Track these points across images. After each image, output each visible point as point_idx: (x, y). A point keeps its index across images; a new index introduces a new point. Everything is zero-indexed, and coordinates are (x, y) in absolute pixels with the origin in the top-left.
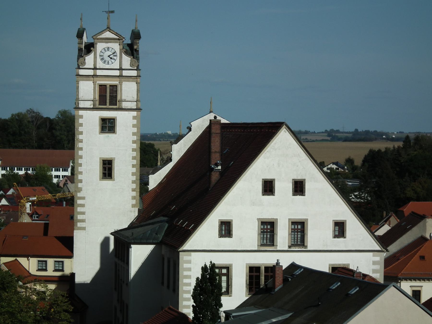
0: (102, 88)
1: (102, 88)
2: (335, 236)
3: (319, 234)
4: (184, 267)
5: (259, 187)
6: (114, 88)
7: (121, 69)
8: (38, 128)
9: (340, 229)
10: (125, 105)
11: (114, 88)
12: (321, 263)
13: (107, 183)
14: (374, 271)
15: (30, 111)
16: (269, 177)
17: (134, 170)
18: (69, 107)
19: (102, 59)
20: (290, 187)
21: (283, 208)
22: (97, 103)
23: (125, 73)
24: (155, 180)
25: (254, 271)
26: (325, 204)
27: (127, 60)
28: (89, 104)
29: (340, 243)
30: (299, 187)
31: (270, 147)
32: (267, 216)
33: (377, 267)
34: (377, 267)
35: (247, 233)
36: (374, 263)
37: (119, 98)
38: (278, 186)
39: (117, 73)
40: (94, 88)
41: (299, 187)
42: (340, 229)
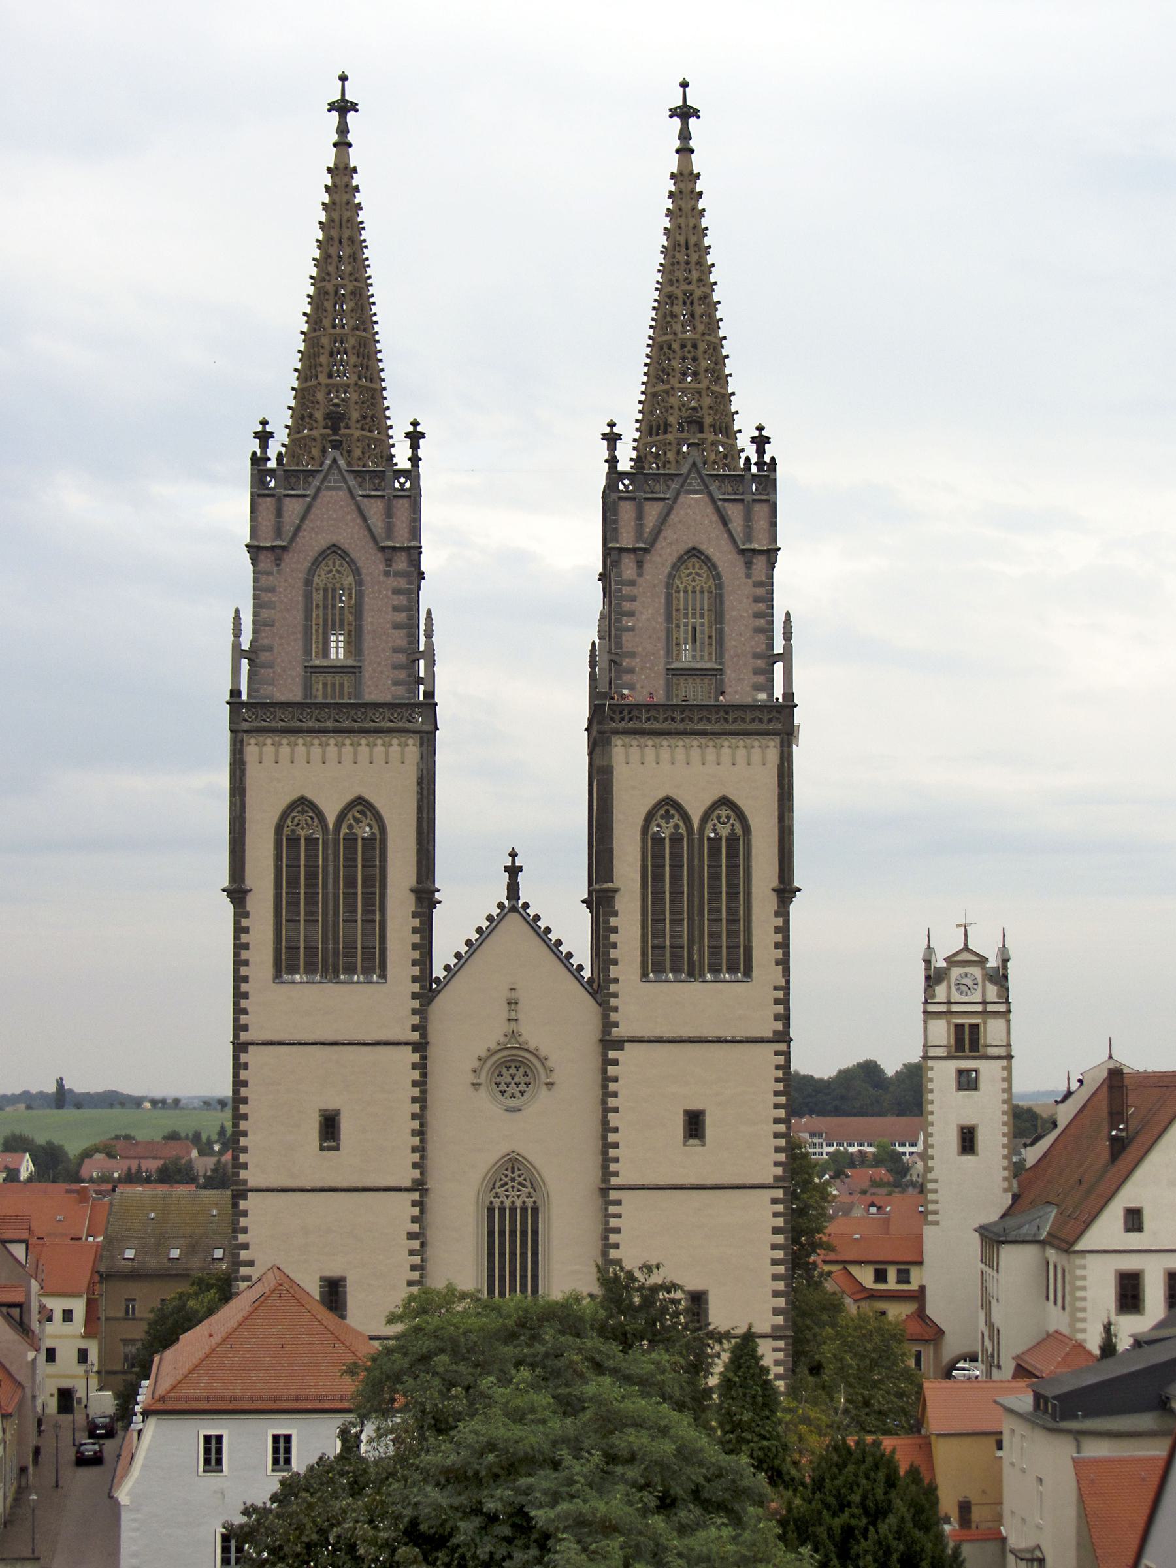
0: (959, 1028)
1: (959, 1028)
6: (975, 1028)
7: (984, 1003)
11: (975, 1028)
17: (1006, 1140)
22: (953, 1049)
23: (990, 1008)
24: (1032, 1155)
27: (992, 991)
37: (982, 1042)
39: (979, 1008)
40: (948, 1029)
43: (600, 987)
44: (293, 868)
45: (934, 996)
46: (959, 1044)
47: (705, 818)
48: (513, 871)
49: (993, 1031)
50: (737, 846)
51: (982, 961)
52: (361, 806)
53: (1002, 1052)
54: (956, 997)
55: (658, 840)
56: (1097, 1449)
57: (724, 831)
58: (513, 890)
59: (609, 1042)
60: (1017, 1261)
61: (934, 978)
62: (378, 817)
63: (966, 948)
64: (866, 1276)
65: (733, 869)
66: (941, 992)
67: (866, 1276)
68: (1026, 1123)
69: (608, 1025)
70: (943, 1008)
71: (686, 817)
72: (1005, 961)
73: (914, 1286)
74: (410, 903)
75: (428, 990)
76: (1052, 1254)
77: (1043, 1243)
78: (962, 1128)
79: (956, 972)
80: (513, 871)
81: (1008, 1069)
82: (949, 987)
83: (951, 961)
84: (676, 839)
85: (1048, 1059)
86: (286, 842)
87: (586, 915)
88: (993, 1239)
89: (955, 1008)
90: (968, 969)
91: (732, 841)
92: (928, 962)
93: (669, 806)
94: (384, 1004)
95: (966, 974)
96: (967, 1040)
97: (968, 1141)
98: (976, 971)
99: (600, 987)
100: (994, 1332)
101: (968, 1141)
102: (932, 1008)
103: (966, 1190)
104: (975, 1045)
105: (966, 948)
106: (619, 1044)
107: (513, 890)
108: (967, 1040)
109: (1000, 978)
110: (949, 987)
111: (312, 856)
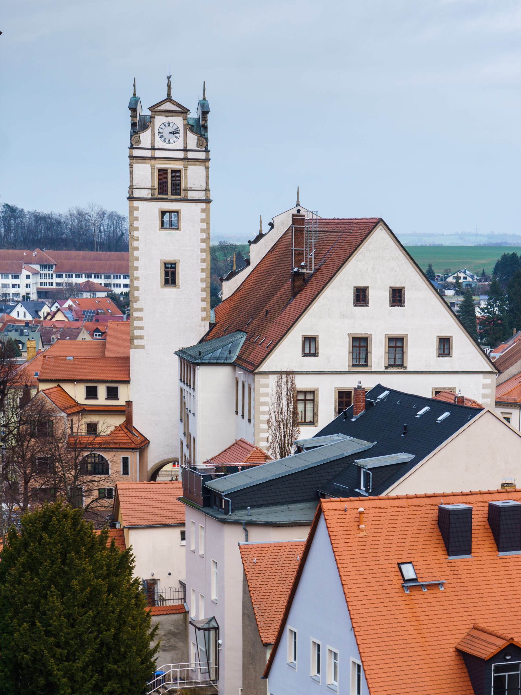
0: (162, 172)
1: (162, 172)
2: (440, 356)
3: (420, 353)
4: (261, 392)
5: (351, 295)
7: (185, 150)
9: (445, 346)
10: (191, 195)
11: (176, 173)
12: (421, 387)
13: (170, 291)
14: (484, 396)
16: (362, 284)
17: (204, 275)
19: (162, 137)
20: (387, 295)
21: (379, 321)
22: (157, 192)
23: (190, 155)
24: (228, 289)
25: (344, 397)
26: (427, 318)
27: (192, 140)
28: (146, 194)
29: (445, 364)
30: (397, 297)
31: (363, 247)
32: (360, 331)
33: (488, 391)
34: (488, 391)
35: (336, 352)
36: (485, 386)
37: (183, 186)
38: (372, 295)
39: (181, 155)
40: (153, 173)
41: (397, 297)
42: (445, 346)
45: (138, 142)
46: (162, 188)
49: (193, 177)
51: (183, 111)
53: (202, 196)
54: (159, 143)
56: (260, 537)
60: (213, 381)
61: (139, 126)
63: (169, 99)
64: (78, 393)
66: (145, 138)
67: (78, 393)
68: (224, 260)
70: (148, 153)
72: (205, 114)
73: (122, 401)
76: (240, 373)
77: (233, 365)
78: (165, 264)
79: (159, 120)
81: (206, 211)
82: (153, 135)
83: (155, 110)
85: (247, 204)
88: (190, 361)
89: (158, 154)
90: (171, 119)
92: (133, 110)
95: (169, 123)
96: (169, 184)
97: (170, 275)
98: (178, 122)
100: (190, 441)
101: (170, 275)
102: (136, 153)
103: (169, 319)
104: (177, 189)
105: (169, 99)
108: (169, 184)
109: (199, 128)
110: (153, 135)
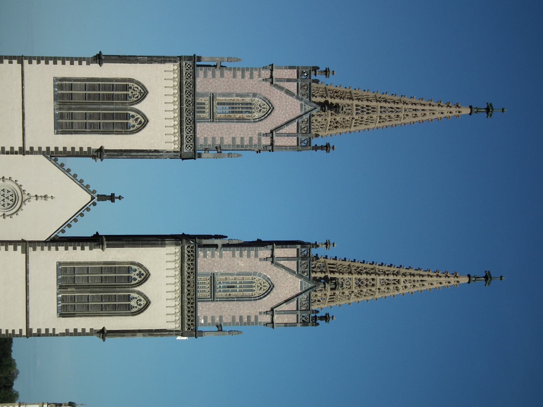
8: (6, 378)
15: (17, 372)
18: (21, 399)
43: (56, 241)
44: (112, 88)
47: (139, 293)
48: (112, 198)
50: (125, 309)
52: (144, 123)
55: (129, 270)
57: (133, 303)
58: (102, 198)
59: (26, 245)
62: (138, 130)
65: (115, 307)
69: (34, 244)
71: (140, 283)
74: (96, 146)
75: (53, 155)
80: (112, 198)
84: (129, 279)
86: (125, 85)
87: (90, 234)
91: (129, 307)
93: (145, 277)
94: (43, 131)
99: (56, 241)
106: (25, 251)
107: (102, 198)
111: (118, 97)
